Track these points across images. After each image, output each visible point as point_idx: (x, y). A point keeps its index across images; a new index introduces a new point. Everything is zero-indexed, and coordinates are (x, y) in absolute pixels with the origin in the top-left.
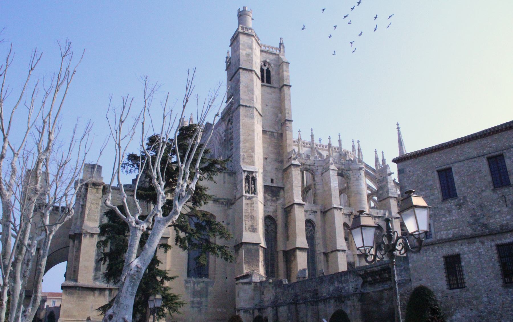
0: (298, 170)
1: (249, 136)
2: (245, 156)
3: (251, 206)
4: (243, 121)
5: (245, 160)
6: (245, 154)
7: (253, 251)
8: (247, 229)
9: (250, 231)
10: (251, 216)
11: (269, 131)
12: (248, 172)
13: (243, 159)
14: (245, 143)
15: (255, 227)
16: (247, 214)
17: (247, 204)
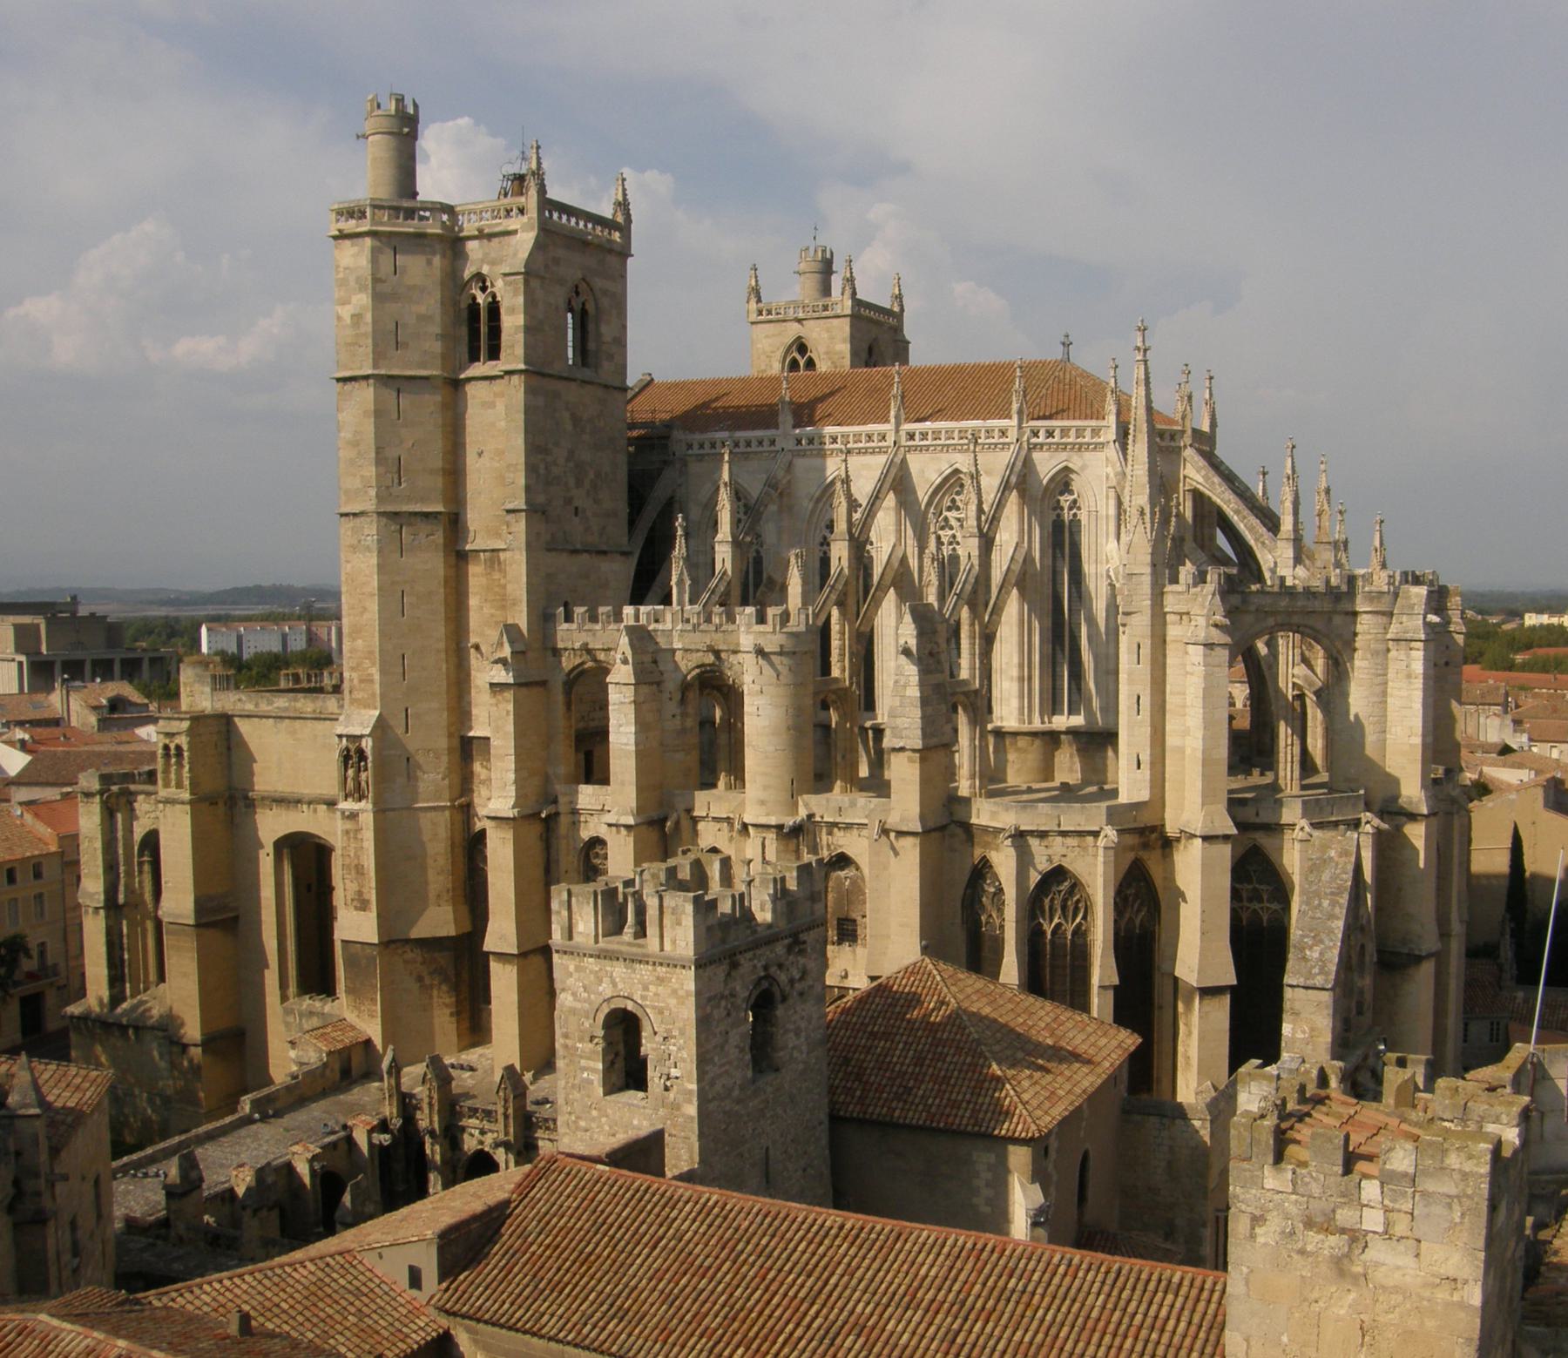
0: (508, 701)
1: (362, 613)
2: (356, 682)
3: (356, 838)
4: (349, 566)
5: (358, 695)
6: (354, 675)
7: (364, 961)
8: (349, 902)
9: (356, 908)
10: (356, 866)
11: (484, 551)
12: (348, 737)
13: (350, 692)
14: (354, 640)
15: (366, 897)
16: (347, 861)
17: (347, 832)
